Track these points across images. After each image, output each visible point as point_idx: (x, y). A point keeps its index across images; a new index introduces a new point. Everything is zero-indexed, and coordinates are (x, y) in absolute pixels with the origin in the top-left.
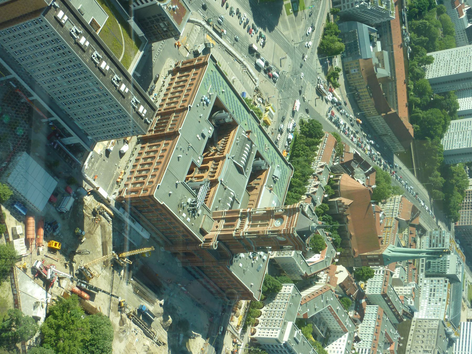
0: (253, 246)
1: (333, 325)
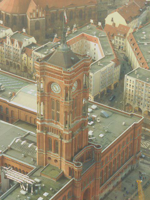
0: (81, 120)
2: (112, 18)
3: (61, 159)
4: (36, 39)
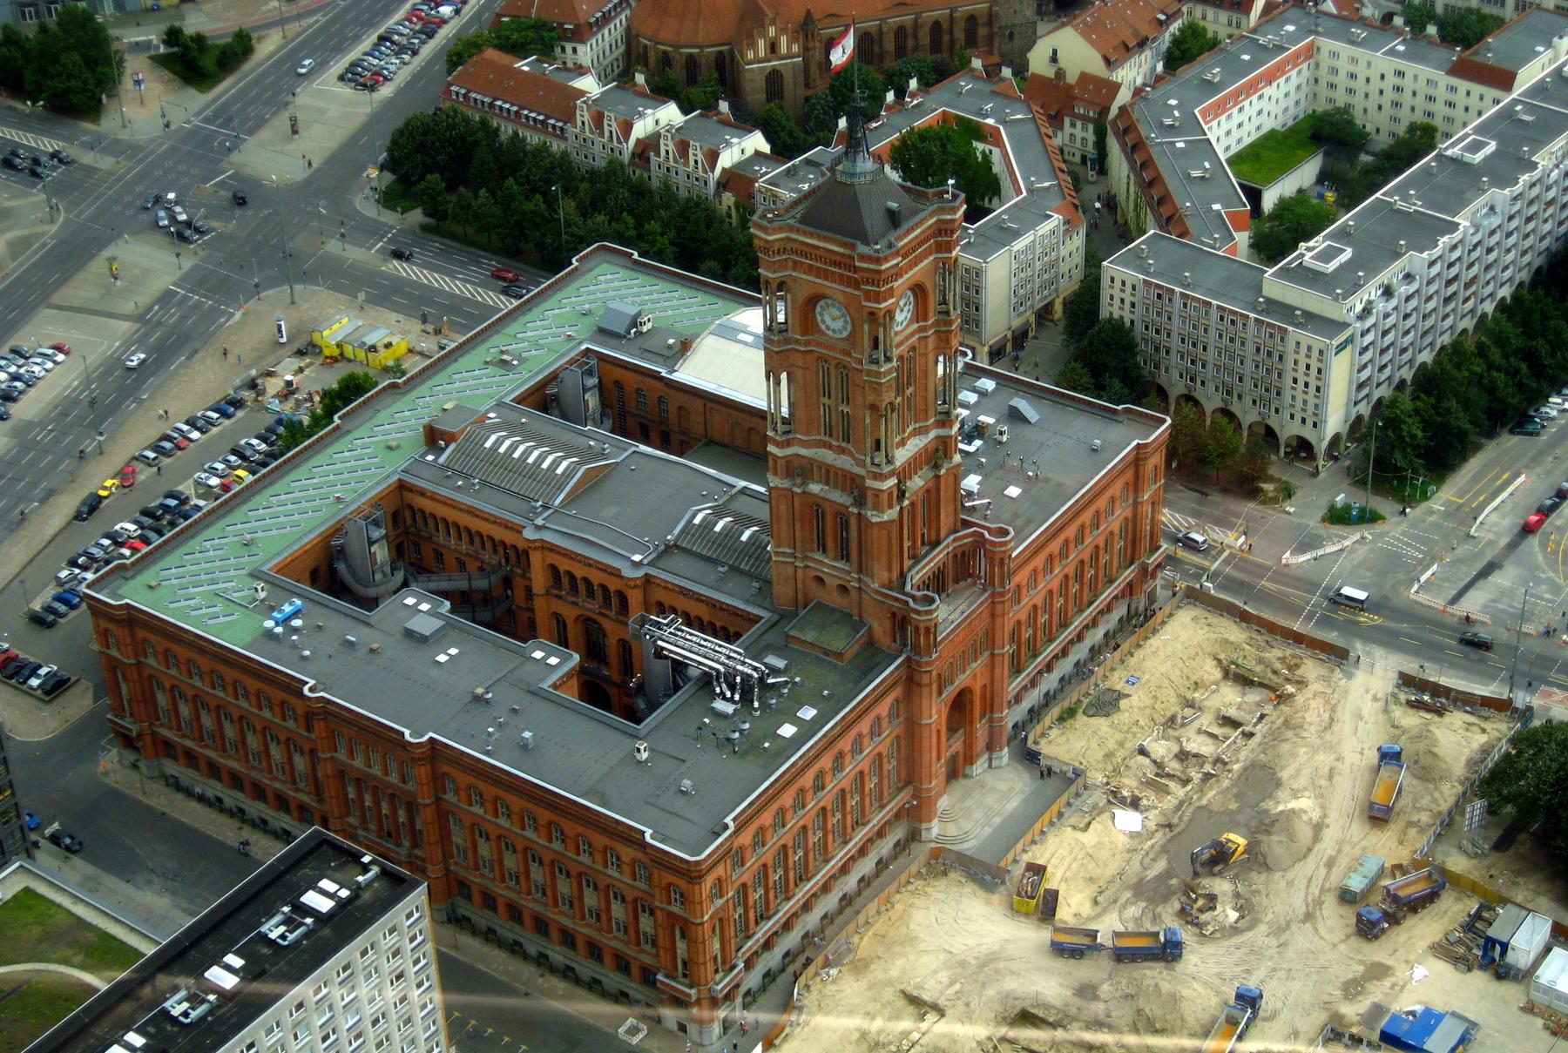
0: (932, 434)
1: (1283, 104)
2: (1055, 52)
3: (859, 580)
4: (768, 138)
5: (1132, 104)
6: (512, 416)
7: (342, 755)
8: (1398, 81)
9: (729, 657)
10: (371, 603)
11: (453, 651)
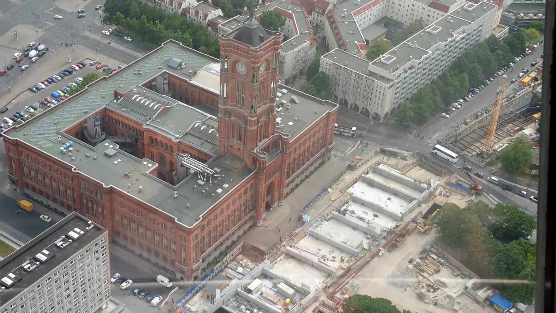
0: (268, 105)
1: (378, 12)
4: (223, 11)
5: (333, 10)
6: (141, 90)
7: (83, 190)
8: (413, 8)
9: (203, 168)
10: (94, 144)
11: (119, 160)
